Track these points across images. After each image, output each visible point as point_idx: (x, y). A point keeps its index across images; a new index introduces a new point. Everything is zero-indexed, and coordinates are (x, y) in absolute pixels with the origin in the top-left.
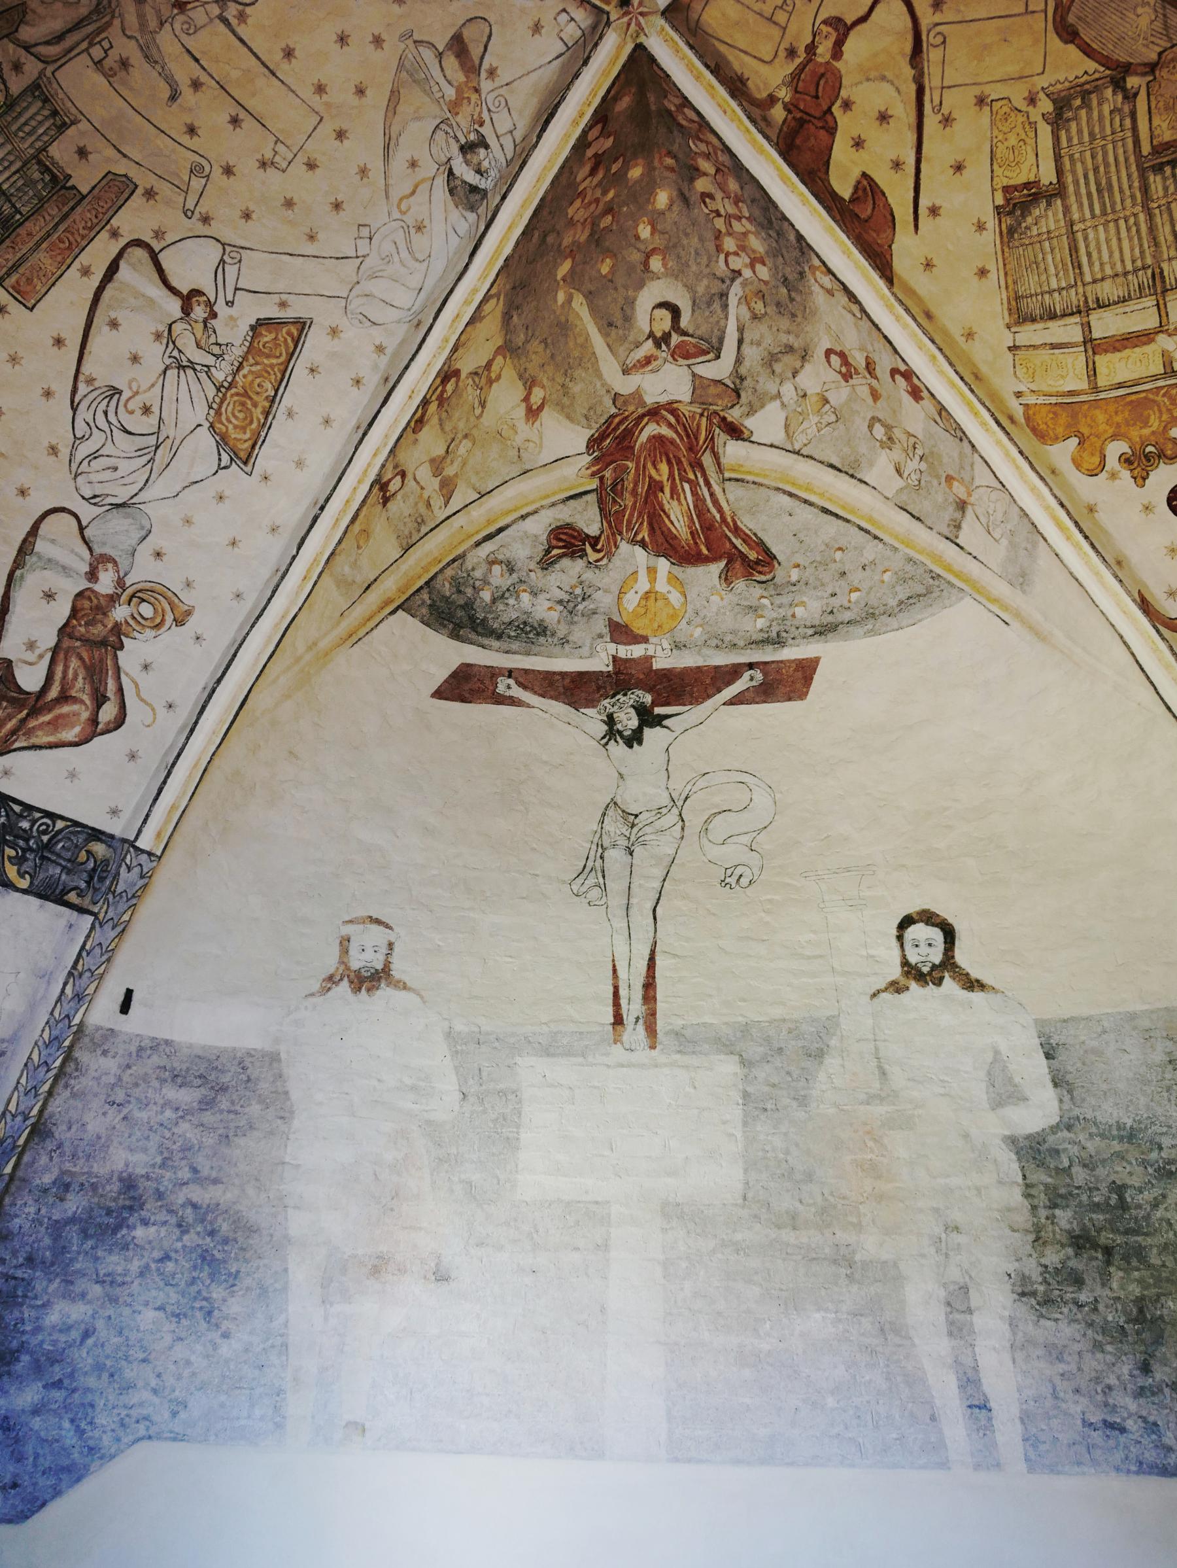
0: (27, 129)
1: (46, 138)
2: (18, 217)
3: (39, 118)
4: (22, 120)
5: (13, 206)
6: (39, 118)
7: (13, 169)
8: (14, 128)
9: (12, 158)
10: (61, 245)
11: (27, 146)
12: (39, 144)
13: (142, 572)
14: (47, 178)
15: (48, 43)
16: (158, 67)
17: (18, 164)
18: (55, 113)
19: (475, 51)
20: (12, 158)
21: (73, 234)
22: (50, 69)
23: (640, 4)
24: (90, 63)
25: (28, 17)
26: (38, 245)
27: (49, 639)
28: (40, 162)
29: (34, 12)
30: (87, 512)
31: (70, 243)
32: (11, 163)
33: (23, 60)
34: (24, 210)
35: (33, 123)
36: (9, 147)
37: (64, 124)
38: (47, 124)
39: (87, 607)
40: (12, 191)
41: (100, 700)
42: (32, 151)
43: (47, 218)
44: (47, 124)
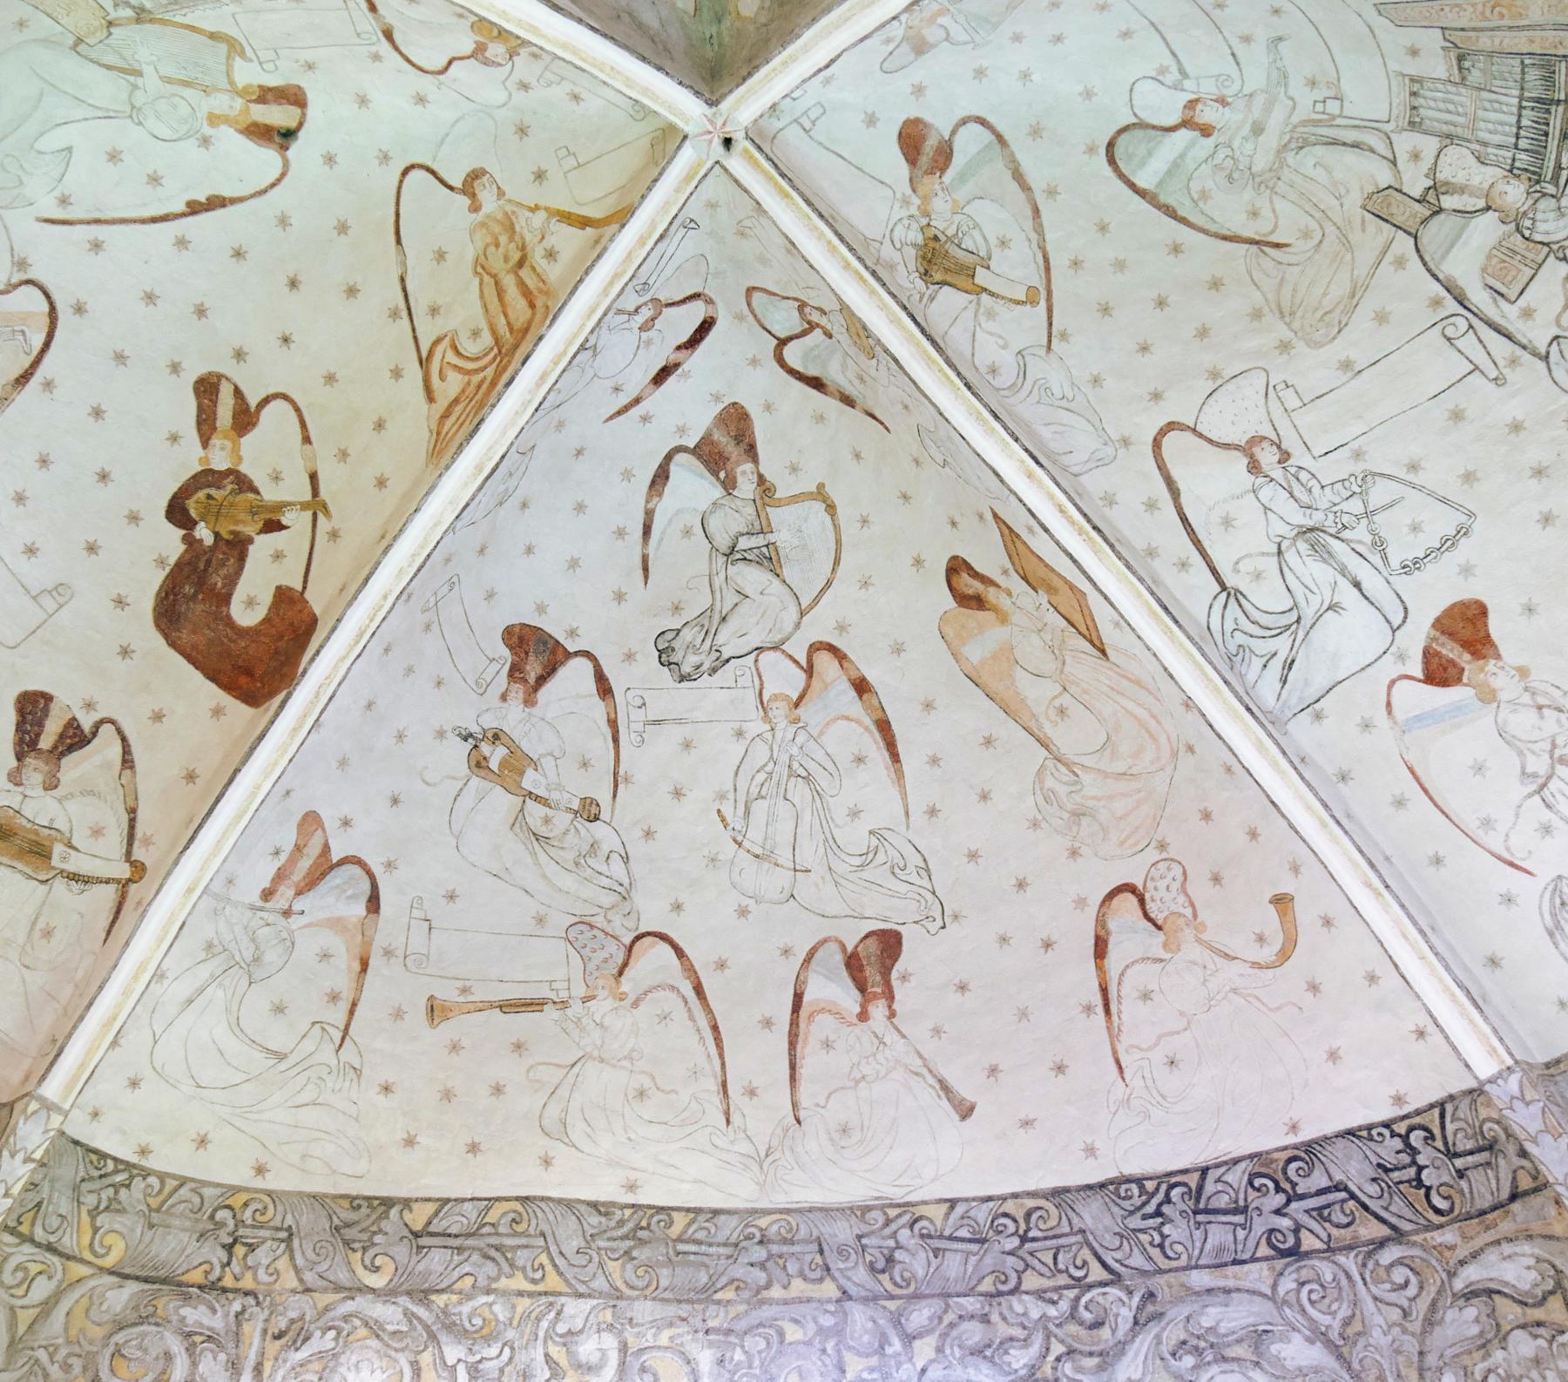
0: (1451, 107)
1: (1440, 87)
2: (1527, 62)
3: (1432, 103)
4: (1448, 117)
5: (1523, 73)
6: (1432, 103)
7: (1493, 96)
8: (1461, 120)
9: (1487, 105)
10: (1505, 11)
11: (1464, 97)
12: (1450, 88)
14: (1467, 64)
15: (1373, 151)
16: (1279, 64)
17: (1485, 95)
18: (1414, 94)
19: (905, 48)
20: (1487, 105)
21: (1483, 13)
22: (1388, 127)
23: (711, 142)
24: (1346, 104)
25: (1371, 189)
26: (1529, 27)
28: (1463, 79)
29: (1362, 189)
31: (1493, 8)
32: (1491, 101)
33: (1406, 156)
34: (1516, 62)
35: (1441, 106)
36: (1480, 113)
37: (1412, 80)
38: (1429, 94)
40: (1511, 84)
42: (1463, 90)
43: (1497, 42)
44: (1429, 94)
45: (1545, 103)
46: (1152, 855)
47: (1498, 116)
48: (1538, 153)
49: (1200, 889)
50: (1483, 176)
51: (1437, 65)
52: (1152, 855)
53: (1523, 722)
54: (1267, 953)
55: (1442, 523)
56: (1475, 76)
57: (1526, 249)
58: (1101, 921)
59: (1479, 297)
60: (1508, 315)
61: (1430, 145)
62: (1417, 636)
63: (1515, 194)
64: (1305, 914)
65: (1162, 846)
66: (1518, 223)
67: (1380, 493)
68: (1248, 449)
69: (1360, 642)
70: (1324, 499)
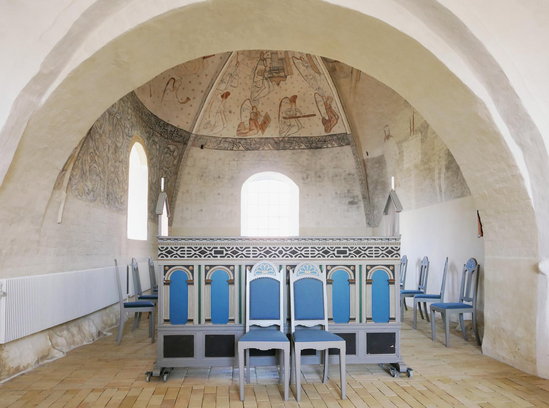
11: (277, 60)
13: (326, 95)
27: (325, 111)
30: (317, 92)
39: (326, 104)
41: (335, 115)
45: (278, 70)
46: (179, 78)
47: (275, 64)
48: (273, 70)
49: (181, 88)
50: (268, 64)
51: (280, 56)
52: (179, 78)
53: (222, 106)
54: (181, 101)
55: (235, 85)
56: (280, 61)
57: (262, 73)
58: (169, 81)
59: (257, 71)
60: (256, 75)
61: (270, 57)
62: (225, 91)
63: (268, 69)
64: (189, 103)
65: (181, 79)
66: (265, 70)
67: (237, 77)
68: (238, 62)
69: (223, 88)
70: (235, 73)
